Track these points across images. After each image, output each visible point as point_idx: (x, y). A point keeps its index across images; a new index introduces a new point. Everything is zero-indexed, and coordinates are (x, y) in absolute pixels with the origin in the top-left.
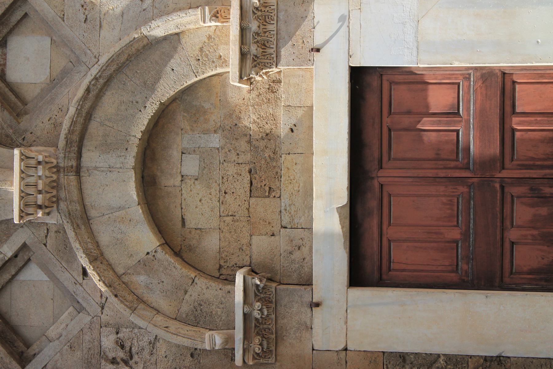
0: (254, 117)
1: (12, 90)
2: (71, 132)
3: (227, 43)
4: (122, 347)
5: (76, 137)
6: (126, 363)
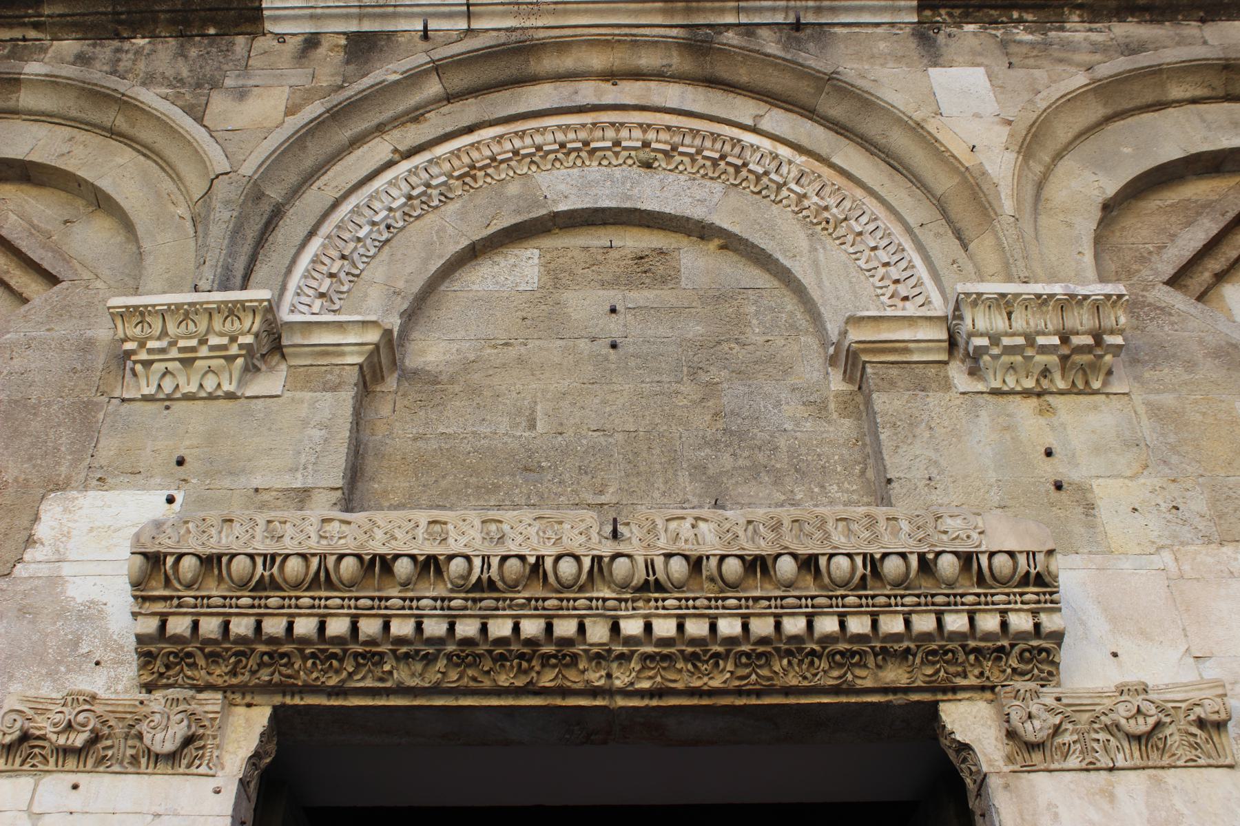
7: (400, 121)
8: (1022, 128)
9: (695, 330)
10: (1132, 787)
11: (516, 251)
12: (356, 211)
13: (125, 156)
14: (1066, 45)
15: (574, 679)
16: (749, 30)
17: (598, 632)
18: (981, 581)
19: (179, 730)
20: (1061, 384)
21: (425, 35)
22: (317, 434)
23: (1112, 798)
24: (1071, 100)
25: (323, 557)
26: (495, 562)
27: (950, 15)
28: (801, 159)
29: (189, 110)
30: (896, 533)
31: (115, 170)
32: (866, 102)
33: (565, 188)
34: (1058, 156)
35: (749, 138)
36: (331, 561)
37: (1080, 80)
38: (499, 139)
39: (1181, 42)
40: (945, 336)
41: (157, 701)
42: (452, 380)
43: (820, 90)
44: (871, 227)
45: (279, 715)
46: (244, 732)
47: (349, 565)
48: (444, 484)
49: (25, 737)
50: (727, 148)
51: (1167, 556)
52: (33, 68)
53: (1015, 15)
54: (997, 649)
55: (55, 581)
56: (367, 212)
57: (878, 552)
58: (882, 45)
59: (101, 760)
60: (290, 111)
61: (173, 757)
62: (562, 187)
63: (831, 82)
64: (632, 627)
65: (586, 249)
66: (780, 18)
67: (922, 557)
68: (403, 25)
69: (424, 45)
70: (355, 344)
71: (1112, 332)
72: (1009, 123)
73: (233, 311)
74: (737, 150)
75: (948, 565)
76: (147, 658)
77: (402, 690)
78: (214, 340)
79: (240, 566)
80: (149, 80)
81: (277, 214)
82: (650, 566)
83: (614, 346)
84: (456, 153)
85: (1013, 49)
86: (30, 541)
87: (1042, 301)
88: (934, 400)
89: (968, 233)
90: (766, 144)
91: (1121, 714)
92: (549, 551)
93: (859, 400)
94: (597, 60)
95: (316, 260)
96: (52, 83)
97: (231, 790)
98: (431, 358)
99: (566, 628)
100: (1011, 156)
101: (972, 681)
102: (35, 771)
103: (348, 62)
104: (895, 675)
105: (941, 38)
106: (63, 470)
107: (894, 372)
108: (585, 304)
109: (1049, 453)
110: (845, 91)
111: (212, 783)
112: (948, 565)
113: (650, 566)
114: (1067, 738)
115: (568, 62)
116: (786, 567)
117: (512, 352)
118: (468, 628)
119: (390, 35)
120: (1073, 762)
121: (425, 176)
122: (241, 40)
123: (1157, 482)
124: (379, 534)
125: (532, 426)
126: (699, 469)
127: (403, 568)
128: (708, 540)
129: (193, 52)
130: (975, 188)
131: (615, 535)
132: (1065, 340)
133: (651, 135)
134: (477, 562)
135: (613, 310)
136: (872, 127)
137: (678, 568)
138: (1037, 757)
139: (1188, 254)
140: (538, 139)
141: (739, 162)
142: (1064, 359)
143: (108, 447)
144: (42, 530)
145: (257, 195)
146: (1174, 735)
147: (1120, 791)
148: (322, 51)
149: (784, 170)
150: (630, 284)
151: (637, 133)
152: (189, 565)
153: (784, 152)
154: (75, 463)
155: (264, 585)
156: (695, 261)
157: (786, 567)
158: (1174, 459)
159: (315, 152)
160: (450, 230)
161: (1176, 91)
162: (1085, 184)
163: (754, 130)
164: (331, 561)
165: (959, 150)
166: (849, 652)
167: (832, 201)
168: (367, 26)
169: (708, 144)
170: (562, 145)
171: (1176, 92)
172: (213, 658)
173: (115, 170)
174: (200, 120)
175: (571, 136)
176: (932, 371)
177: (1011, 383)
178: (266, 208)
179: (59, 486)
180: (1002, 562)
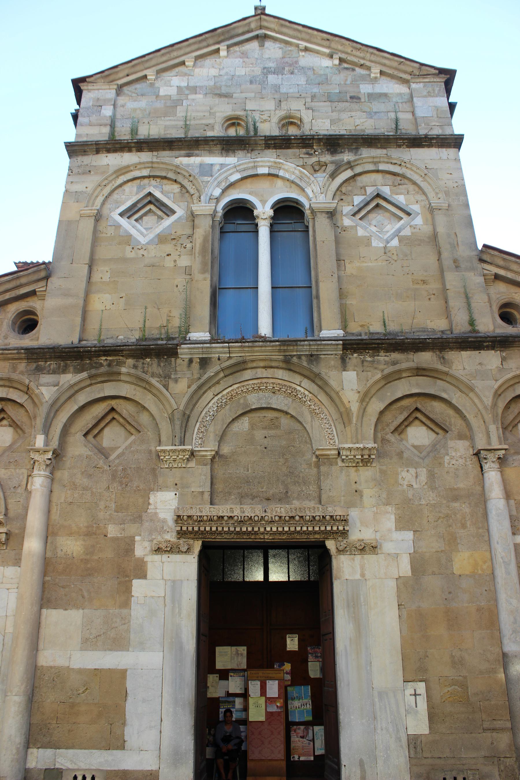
7: (214, 385)
8: (362, 394)
9: (284, 443)
10: (358, 557)
11: (243, 418)
12: (206, 413)
13: (150, 396)
14: (379, 362)
15: (257, 537)
16: (299, 357)
17: (262, 530)
18: (334, 520)
19: (186, 547)
20: (361, 465)
21: (219, 359)
22: (203, 477)
23: (354, 560)
24: (376, 383)
25: (211, 516)
26: (243, 517)
27: (351, 351)
28: (310, 395)
29: (164, 386)
30: (319, 510)
31: (148, 401)
32: (326, 383)
33: (254, 400)
34: (372, 397)
35: (298, 388)
36: (212, 517)
37: (379, 376)
38: (238, 388)
39: (407, 360)
40: (337, 453)
41: (181, 541)
42: (230, 458)
43: (316, 377)
44: (325, 417)
45: (203, 542)
46: (197, 546)
47: (215, 518)
48: (230, 486)
49: (158, 548)
50: (293, 390)
51: (375, 508)
52: (124, 370)
53: (367, 351)
54: (337, 532)
55: (156, 513)
56: (208, 413)
57: (314, 515)
58: (332, 363)
59: (172, 552)
60: (189, 387)
61: (186, 552)
62: (253, 400)
63: (318, 375)
64: (268, 529)
65: (259, 417)
66: (307, 353)
67: (323, 516)
68: (213, 355)
69: (219, 362)
70: (209, 455)
71: (373, 455)
72: (359, 392)
73: (184, 451)
74: (295, 391)
75: (328, 518)
76: (178, 533)
77: (225, 538)
78: (180, 457)
79: (195, 518)
80: (153, 375)
81: (189, 417)
82: (272, 518)
83: (266, 448)
84: (228, 393)
85: (365, 364)
86: (149, 504)
87: (358, 448)
88: (334, 468)
89: (346, 425)
90: (302, 390)
91: (357, 545)
92: (253, 515)
93: (318, 465)
94: (262, 364)
95: (199, 429)
96: (129, 374)
97: (197, 558)
98: (225, 451)
99: (256, 529)
100: (358, 404)
101: (332, 537)
102: (161, 554)
103: (200, 369)
104: (317, 536)
105: (347, 359)
106: (152, 486)
107: (326, 460)
108: (259, 434)
109: (356, 483)
110: (322, 379)
111: (193, 556)
112: (328, 518)
113: (272, 518)
114: (348, 549)
115: (254, 365)
116: (297, 518)
117: (243, 449)
118: (238, 529)
119: (210, 358)
120: (348, 553)
121: (221, 400)
122: (173, 359)
123: (377, 490)
124: (221, 511)
125: (248, 471)
126: (283, 482)
127: (226, 518)
129: (162, 364)
130: (348, 412)
131: (265, 511)
132: (362, 456)
133: (275, 386)
134: (239, 517)
135: (265, 437)
136: (328, 390)
137: (277, 518)
138: (341, 552)
139: (401, 420)
140: (247, 387)
141: (296, 394)
142: (362, 460)
143: (160, 480)
144: (151, 501)
145: (184, 414)
146: (367, 549)
147: (356, 559)
148: (194, 364)
149: (306, 398)
150: (270, 429)
151: (271, 385)
152: (185, 518)
153: (307, 393)
154: (154, 484)
156: (285, 421)
157: (297, 518)
158: (382, 484)
159: (195, 398)
160: (227, 415)
161: (404, 375)
162: (376, 406)
163: (300, 386)
164: (212, 517)
165: (346, 402)
166: (308, 533)
167: (317, 408)
168: (204, 356)
169: (288, 389)
170: (253, 388)
171: (404, 375)
172: (191, 533)
173: (148, 401)
174: (167, 390)
175: (255, 386)
176: (334, 460)
177: (350, 465)
178: (186, 417)
179: (153, 490)
180: (338, 517)
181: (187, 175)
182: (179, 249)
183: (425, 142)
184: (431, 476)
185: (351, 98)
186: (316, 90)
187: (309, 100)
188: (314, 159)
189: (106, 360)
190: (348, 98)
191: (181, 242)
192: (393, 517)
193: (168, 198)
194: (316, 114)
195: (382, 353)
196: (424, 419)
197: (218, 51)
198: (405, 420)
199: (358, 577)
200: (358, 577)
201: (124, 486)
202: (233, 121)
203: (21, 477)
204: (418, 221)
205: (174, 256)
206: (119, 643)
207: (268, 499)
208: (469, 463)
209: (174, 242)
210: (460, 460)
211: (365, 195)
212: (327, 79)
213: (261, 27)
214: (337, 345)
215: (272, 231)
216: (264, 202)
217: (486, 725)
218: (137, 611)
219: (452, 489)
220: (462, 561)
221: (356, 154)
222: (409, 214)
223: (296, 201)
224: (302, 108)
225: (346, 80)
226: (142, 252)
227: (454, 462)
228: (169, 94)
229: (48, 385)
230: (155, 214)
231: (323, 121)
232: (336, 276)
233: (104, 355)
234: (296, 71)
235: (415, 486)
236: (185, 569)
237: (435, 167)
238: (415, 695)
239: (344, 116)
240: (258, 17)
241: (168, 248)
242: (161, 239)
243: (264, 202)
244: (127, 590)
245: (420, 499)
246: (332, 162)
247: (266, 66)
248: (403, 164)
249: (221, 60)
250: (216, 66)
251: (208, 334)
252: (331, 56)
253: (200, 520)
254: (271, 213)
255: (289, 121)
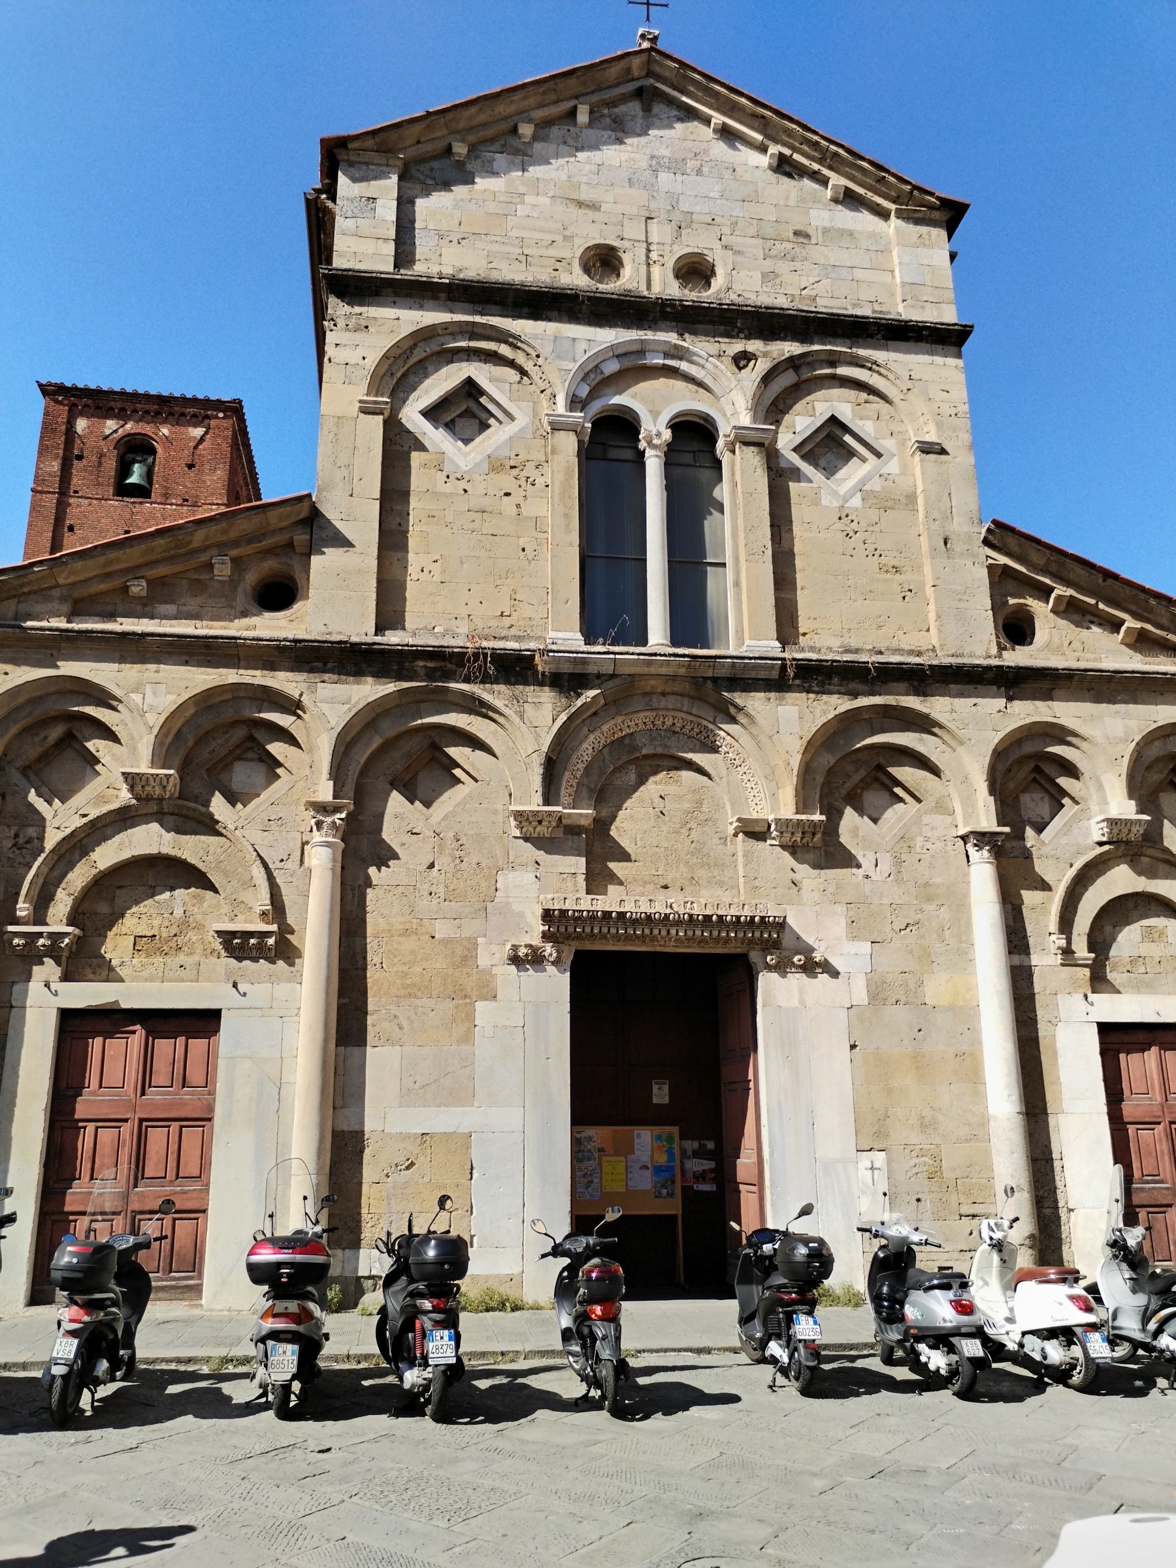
0: (194, 939)
1: (227, 765)
2: (188, 808)
3: (246, 922)
4: (27, 842)
5: (184, 812)
6: (14, 845)
9: (686, 805)
17: (664, 933)
55: (508, 903)
57: (738, 914)
112: (757, 919)
128: (695, 912)
144: (498, 885)
155: (576, 919)
181: (534, 354)
182: (523, 484)
183: (912, 331)
184: (898, 862)
185: (796, 233)
186: (737, 212)
187: (726, 230)
188: (738, 346)
189: (425, 667)
190: (792, 235)
191: (525, 473)
192: (843, 922)
193: (501, 391)
194: (739, 258)
195: (836, 680)
196: (887, 781)
197: (573, 113)
198: (862, 780)
199: (795, 1003)
200: (795, 1003)
201: (458, 861)
202: (604, 260)
203: (291, 844)
204: (892, 467)
205: (517, 496)
206: (459, 1093)
207: (666, 887)
208: (950, 848)
209: (515, 472)
210: (938, 844)
211: (814, 415)
212: (756, 191)
213: (650, 74)
214: (773, 665)
215: (667, 464)
216: (655, 414)
217: (965, 1210)
218: (484, 1048)
219: (926, 884)
220: (936, 989)
221: (802, 341)
222: (878, 455)
223: (707, 419)
224: (717, 245)
225: (788, 198)
226: (463, 484)
227: (929, 845)
228: (492, 188)
229: (332, 701)
230: (474, 416)
231: (751, 274)
232: (769, 552)
233: (421, 659)
234: (705, 169)
235: (874, 878)
236: (554, 986)
237: (924, 378)
238: (872, 1168)
239: (783, 267)
240: (645, 56)
241: (506, 481)
242: (496, 466)
243: (655, 414)
244: (470, 1017)
245: (881, 897)
246: (765, 355)
247: (656, 153)
248: (874, 367)
249: (577, 130)
250: (571, 142)
251: (579, 636)
252: (763, 149)
253: (578, 918)
254: (667, 435)
255: (695, 270)
